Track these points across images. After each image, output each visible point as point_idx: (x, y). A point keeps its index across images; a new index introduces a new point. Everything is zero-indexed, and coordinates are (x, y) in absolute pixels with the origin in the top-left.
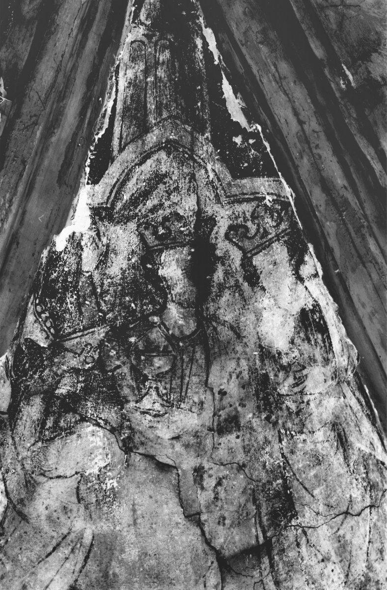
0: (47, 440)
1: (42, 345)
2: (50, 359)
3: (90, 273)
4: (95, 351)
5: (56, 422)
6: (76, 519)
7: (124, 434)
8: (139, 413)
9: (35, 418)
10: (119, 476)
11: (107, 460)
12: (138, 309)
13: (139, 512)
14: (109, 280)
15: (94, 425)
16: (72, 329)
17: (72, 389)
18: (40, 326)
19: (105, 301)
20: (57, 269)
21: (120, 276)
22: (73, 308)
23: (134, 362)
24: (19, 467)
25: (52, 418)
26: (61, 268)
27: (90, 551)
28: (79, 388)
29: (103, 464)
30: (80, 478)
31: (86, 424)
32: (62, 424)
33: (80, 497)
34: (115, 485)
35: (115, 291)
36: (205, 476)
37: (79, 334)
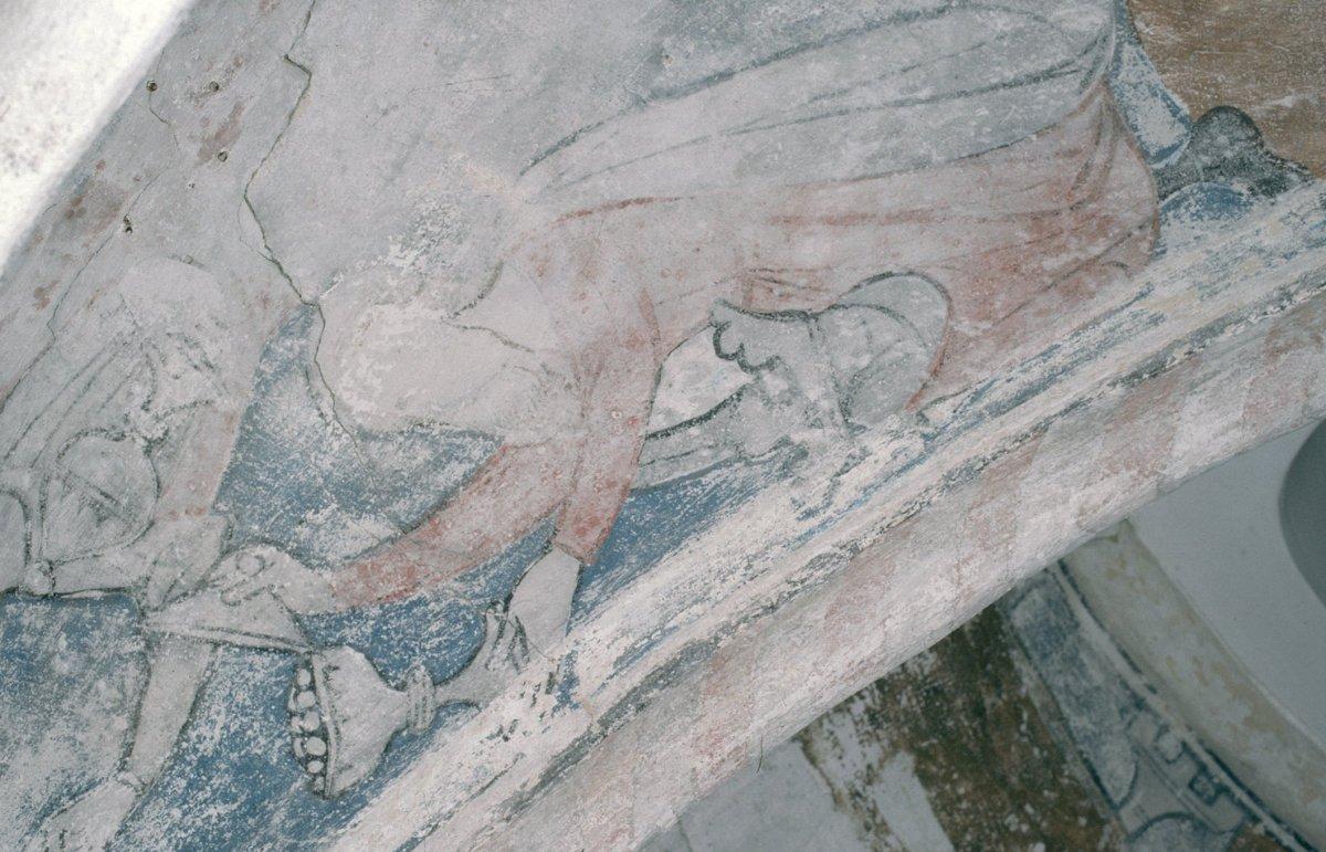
0: (485, 437)
1: (360, 657)
2: (355, 614)
3: (122, 776)
4: (224, 577)
5: (437, 464)
6: (533, 234)
7: (291, 349)
8: (224, 376)
9: (488, 500)
10: (374, 263)
11: (375, 315)
12: (57, 628)
13: (391, 156)
14: (80, 737)
15: (348, 410)
16: (249, 659)
17: (345, 517)
18: (338, 704)
19: (121, 689)
20: (199, 823)
21: (49, 735)
22: (215, 708)
23: (149, 501)
24: (597, 415)
25: (441, 478)
26: (189, 820)
27: (551, 151)
28: (326, 512)
29: (390, 311)
30: (464, 314)
31: (367, 424)
32: (423, 454)
33: (489, 275)
34: (395, 249)
35: (84, 700)
36: (213, 130)
37: (238, 639)
